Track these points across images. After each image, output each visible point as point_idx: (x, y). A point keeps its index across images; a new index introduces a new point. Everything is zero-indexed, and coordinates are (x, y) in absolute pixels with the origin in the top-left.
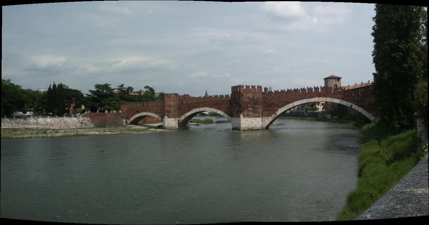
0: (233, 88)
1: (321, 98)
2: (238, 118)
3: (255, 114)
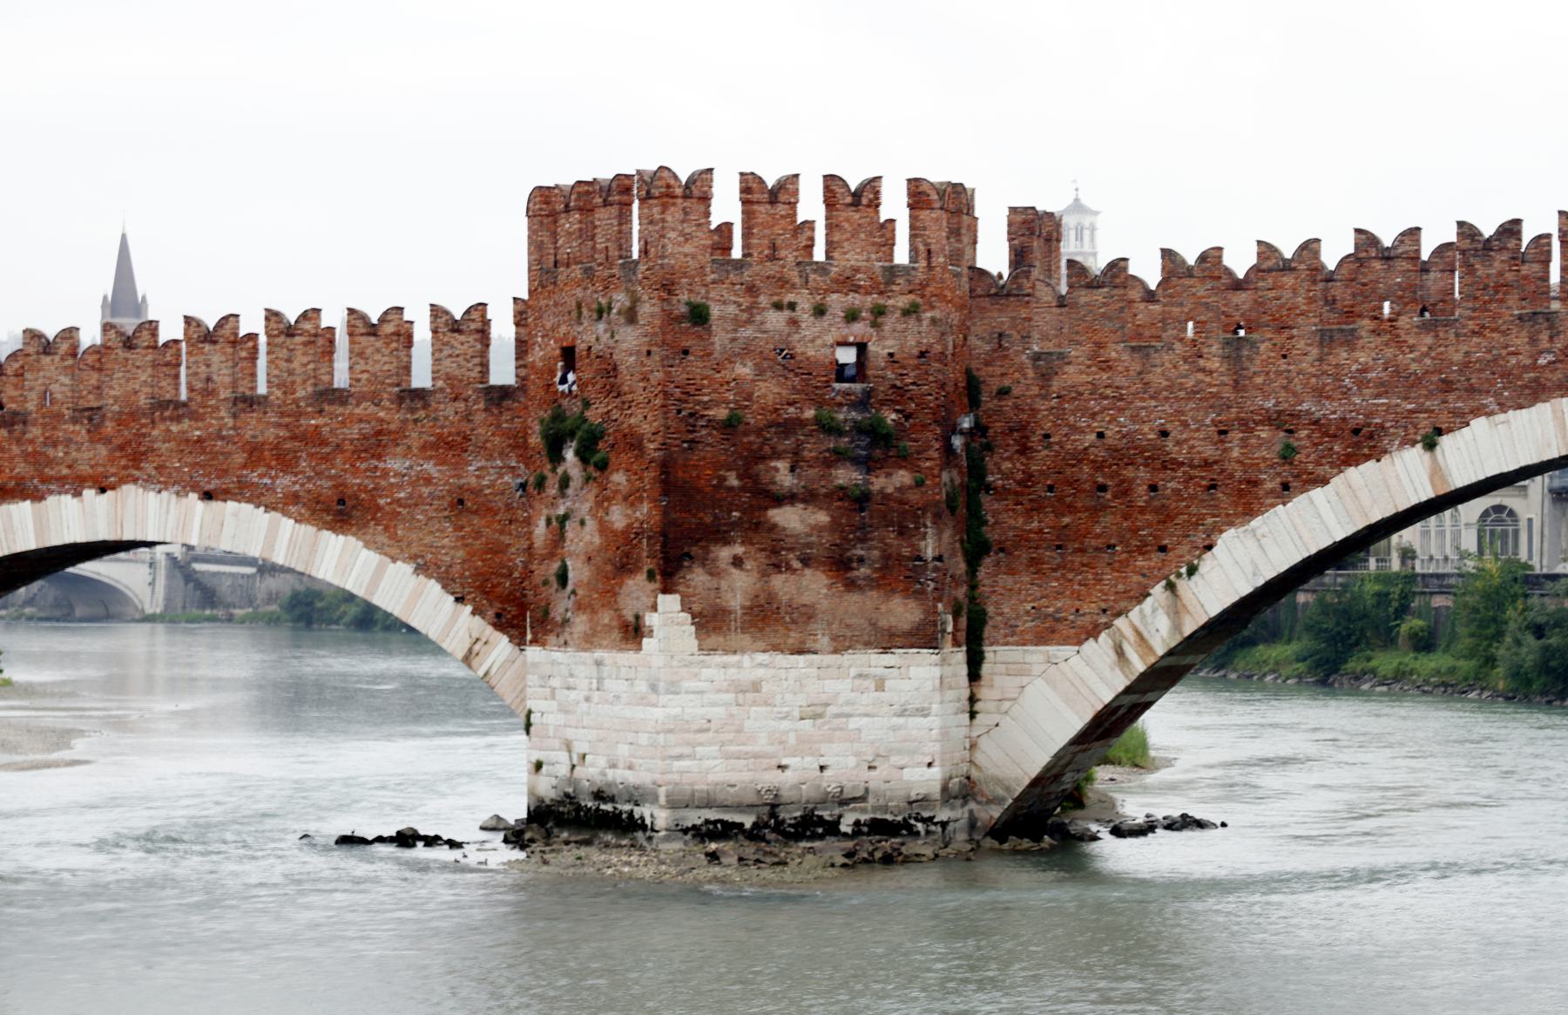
0: (549, 208)
2: (627, 657)
3: (872, 598)
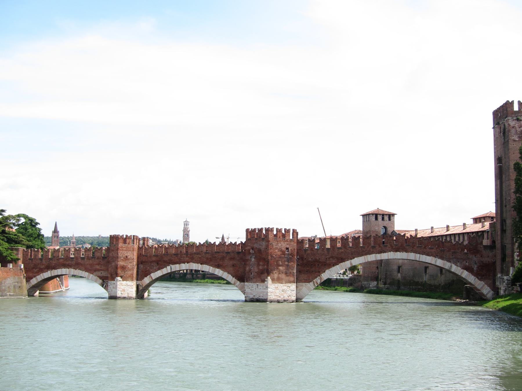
1: (399, 253)
2: (262, 284)
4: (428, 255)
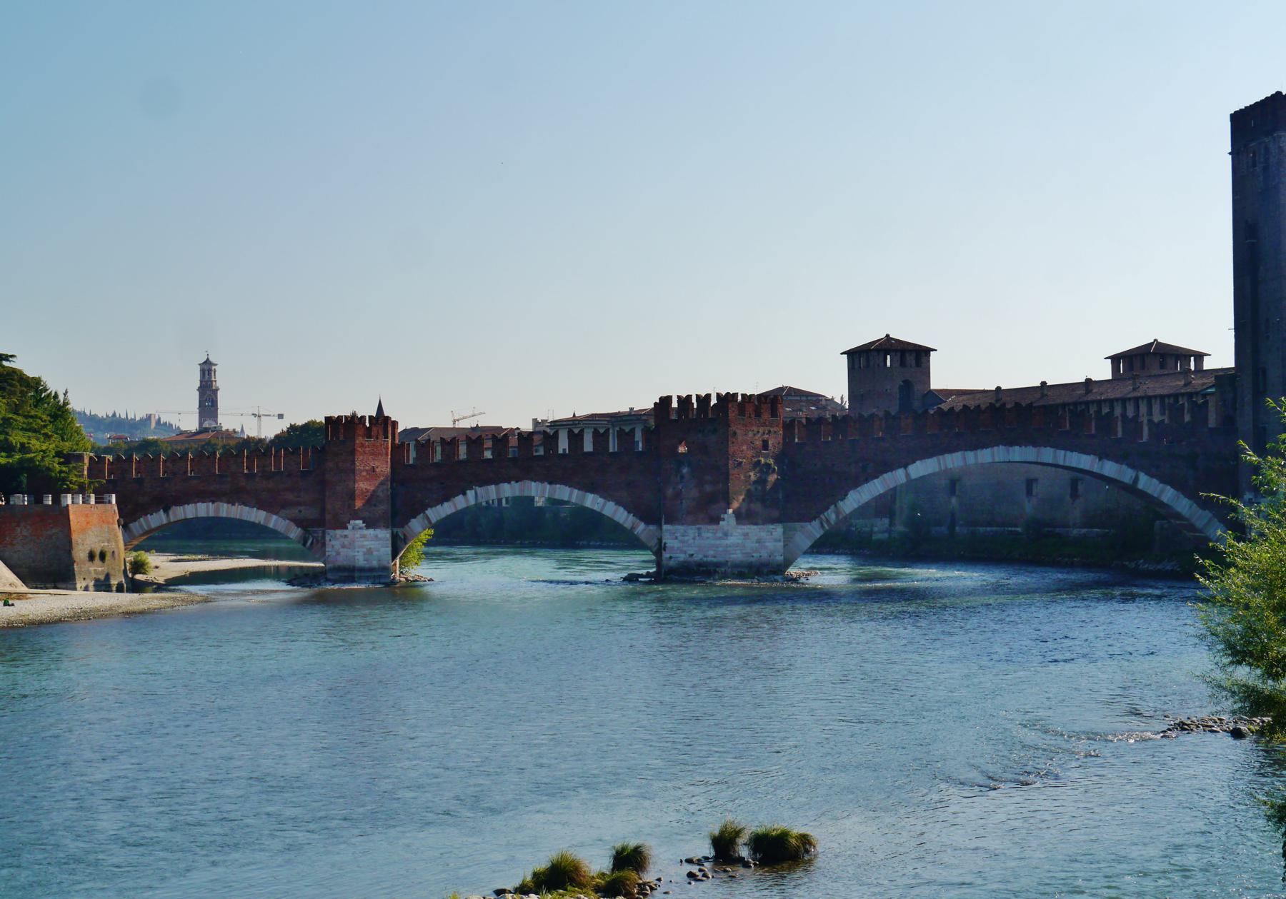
4: (1083, 450)
